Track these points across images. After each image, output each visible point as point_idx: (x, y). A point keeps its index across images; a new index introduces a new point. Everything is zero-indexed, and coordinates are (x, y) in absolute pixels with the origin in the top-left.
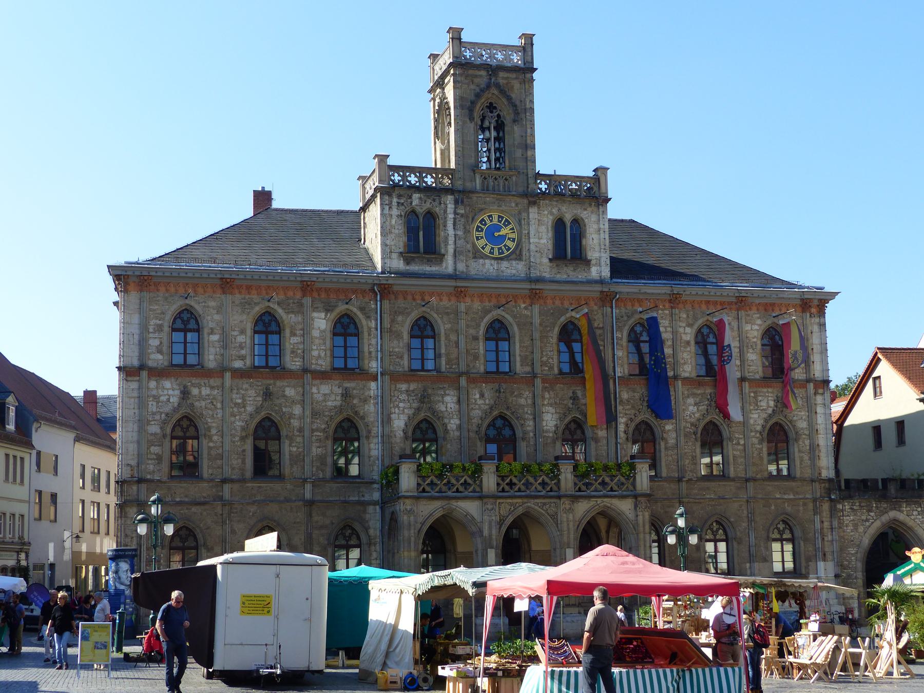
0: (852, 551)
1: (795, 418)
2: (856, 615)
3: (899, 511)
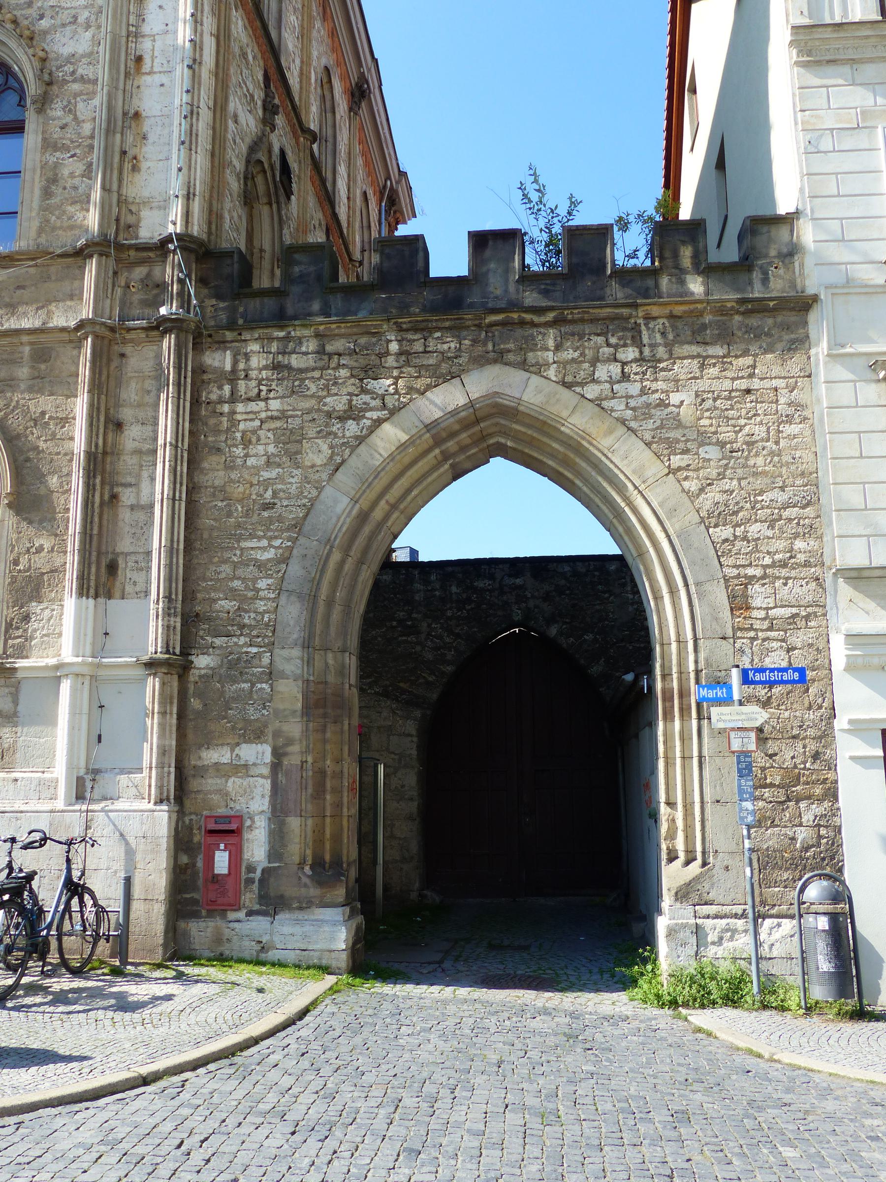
0: (264, 550)
1: (44, 23)
2: (257, 848)
3: (523, 365)
